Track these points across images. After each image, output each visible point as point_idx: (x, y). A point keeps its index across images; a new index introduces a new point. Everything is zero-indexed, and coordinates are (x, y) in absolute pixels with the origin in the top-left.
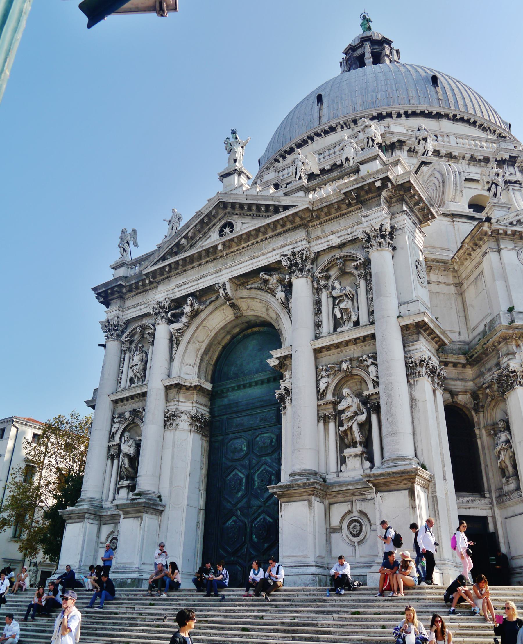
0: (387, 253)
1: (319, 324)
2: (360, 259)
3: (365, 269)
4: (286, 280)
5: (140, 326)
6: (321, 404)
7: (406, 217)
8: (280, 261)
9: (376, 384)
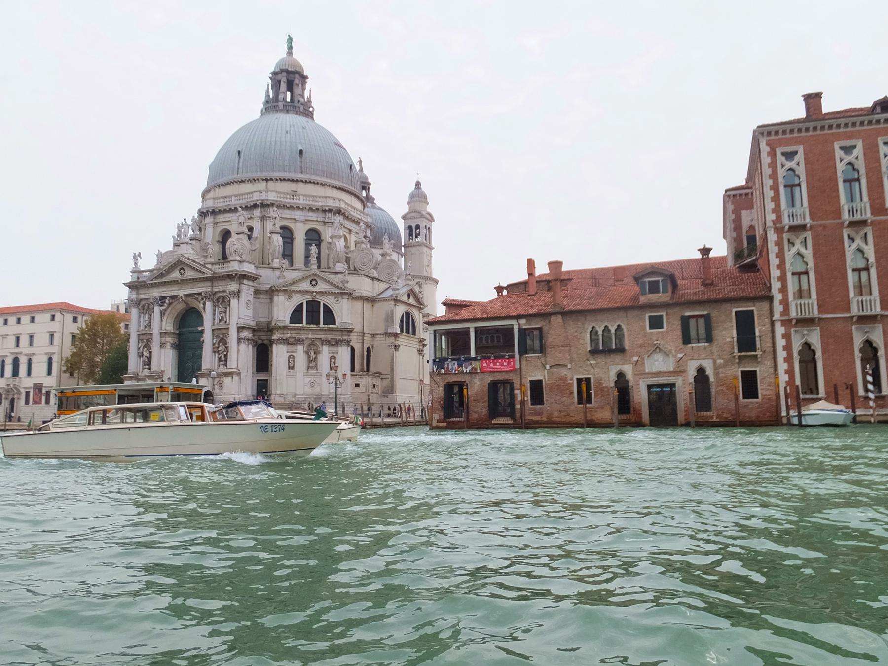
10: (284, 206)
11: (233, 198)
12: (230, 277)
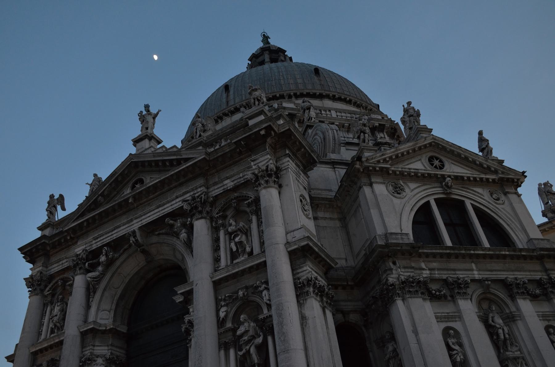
0: (274, 192)
1: (218, 258)
2: (251, 198)
3: (256, 206)
4: (188, 223)
5: (62, 279)
6: (221, 333)
7: (288, 159)
8: (183, 206)
9: (269, 306)
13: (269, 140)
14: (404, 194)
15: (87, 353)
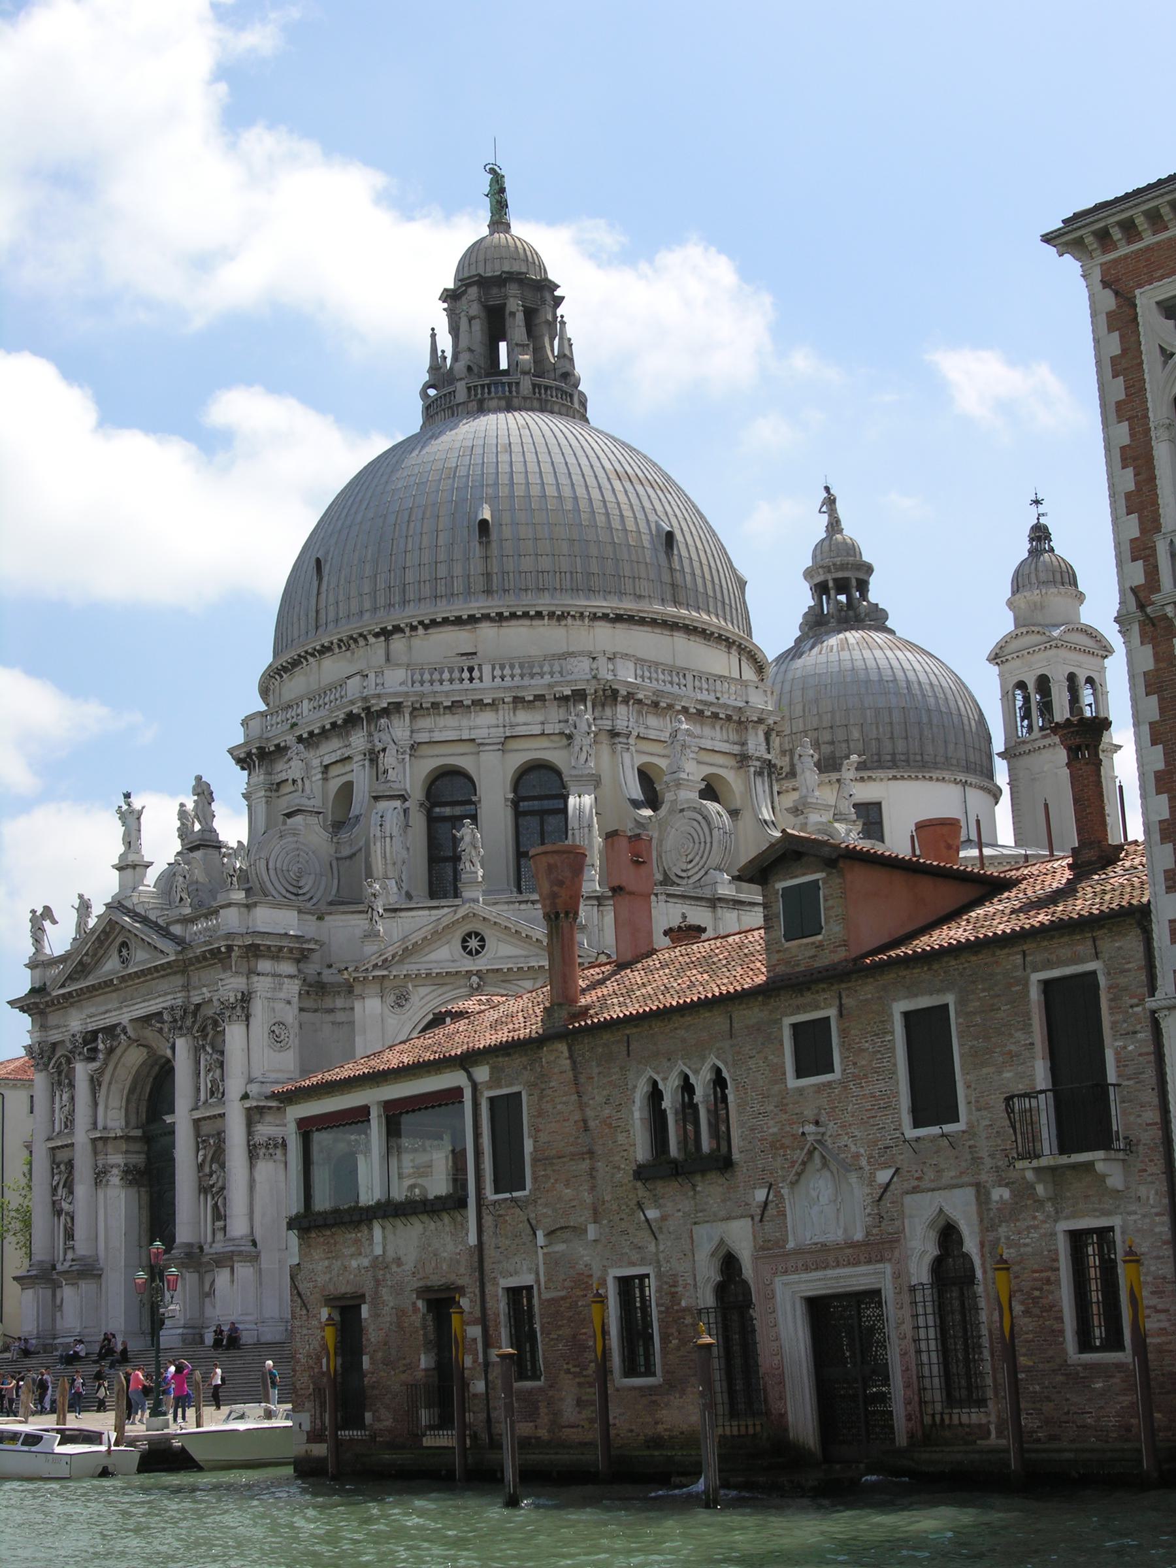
10: (435, 705)
11: (306, 702)
12: (218, 957)
13: (233, 954)
14: (407, 1007)
15: (100, 1163)
